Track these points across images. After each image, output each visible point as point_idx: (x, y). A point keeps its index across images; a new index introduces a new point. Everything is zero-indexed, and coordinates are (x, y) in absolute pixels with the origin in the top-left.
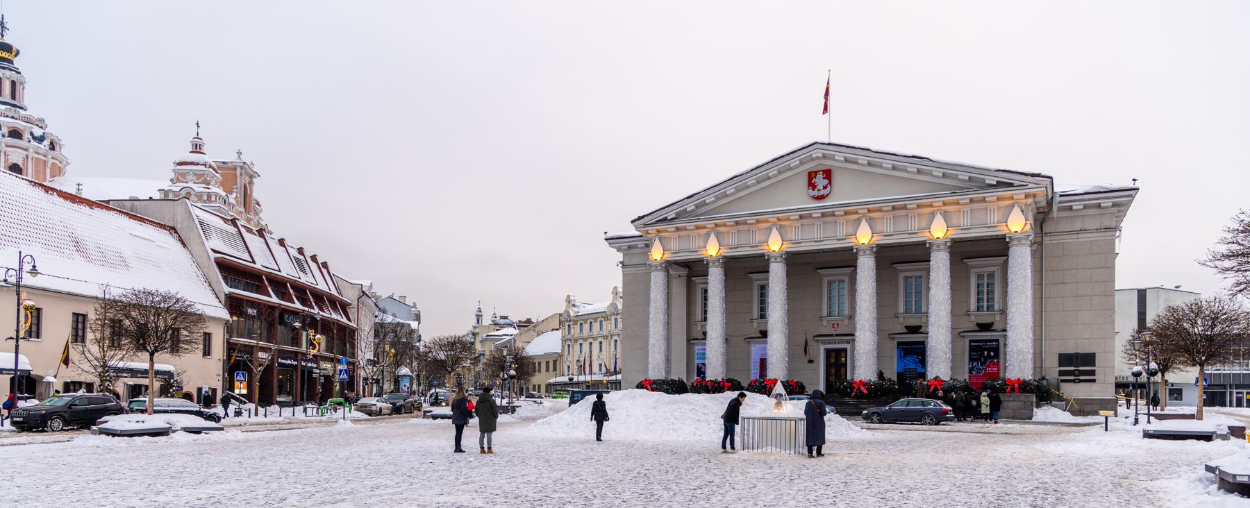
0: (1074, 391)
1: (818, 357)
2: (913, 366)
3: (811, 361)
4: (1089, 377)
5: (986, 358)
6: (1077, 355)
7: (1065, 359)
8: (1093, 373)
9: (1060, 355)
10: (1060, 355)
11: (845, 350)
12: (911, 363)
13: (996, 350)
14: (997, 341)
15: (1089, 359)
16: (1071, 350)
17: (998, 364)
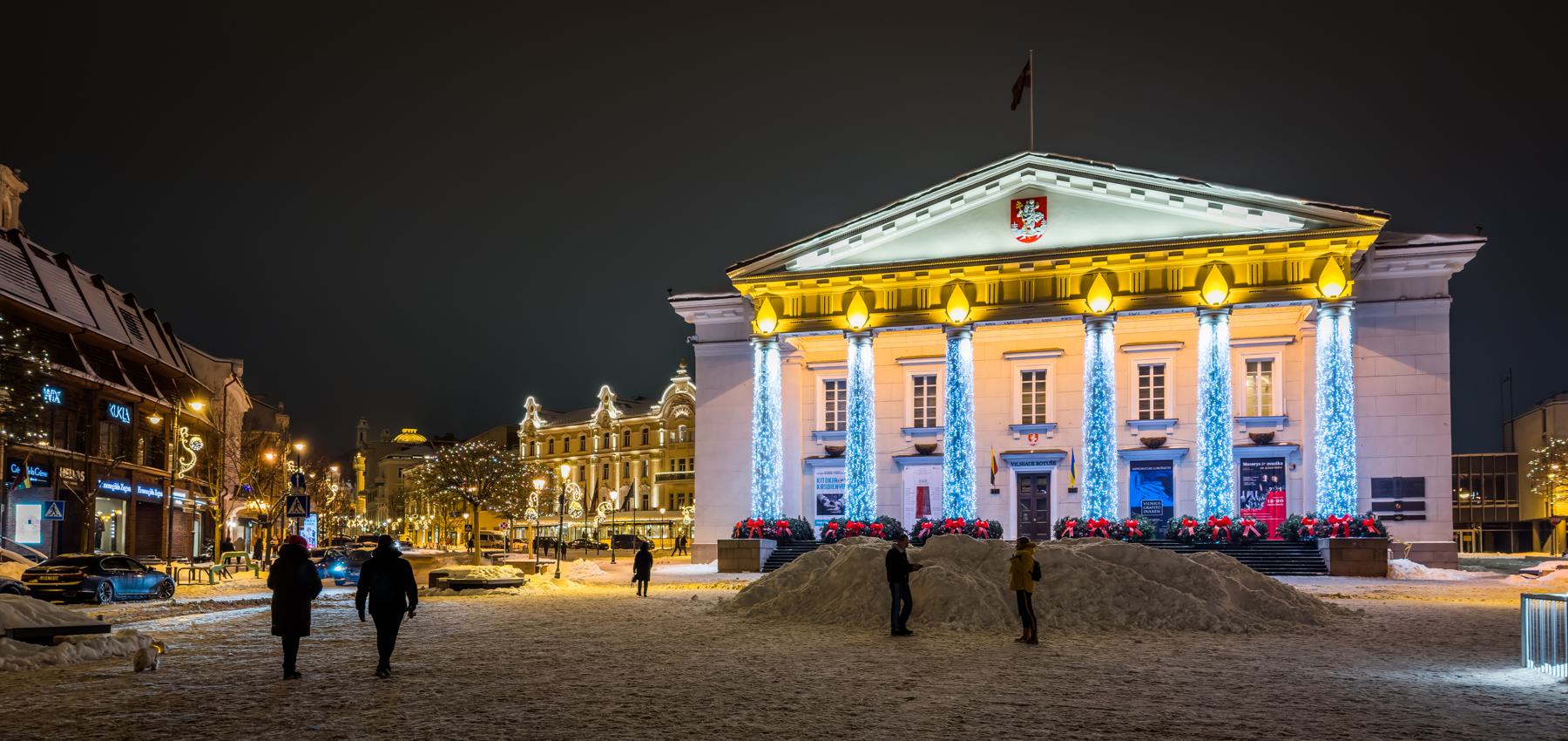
0: (1398, 532)
1: (1007, 485)
2: (1154, 497)
3: (995, 492)
4: (1417, 512)
5: (1266, 486)
6: (1399, 480)
7: (1381, 486)
8: (1422, 506)
9: (1373, 480)
10: (1373, 480)
11: (1047, 476)
12: (1153, 492)
13: (1281, 473)
14: (1282, 459)
15: (1415, 486)
16: (1388, 472)
17: (1283, 494)
